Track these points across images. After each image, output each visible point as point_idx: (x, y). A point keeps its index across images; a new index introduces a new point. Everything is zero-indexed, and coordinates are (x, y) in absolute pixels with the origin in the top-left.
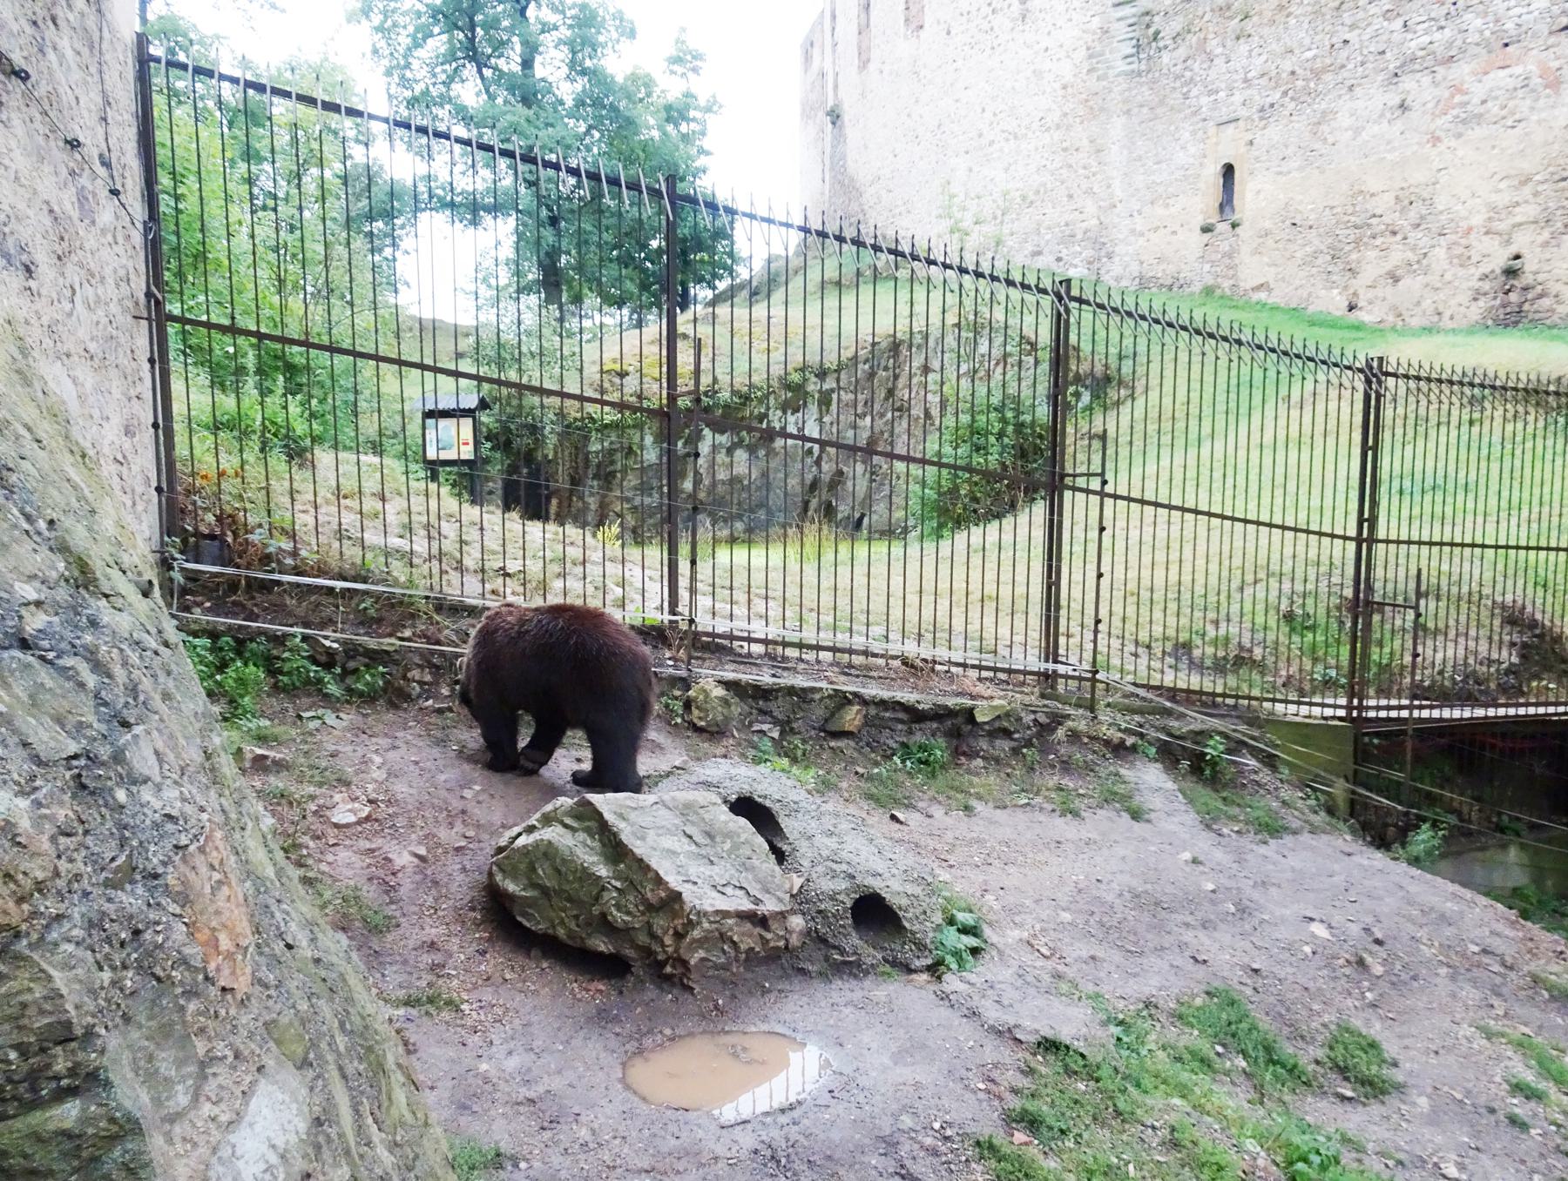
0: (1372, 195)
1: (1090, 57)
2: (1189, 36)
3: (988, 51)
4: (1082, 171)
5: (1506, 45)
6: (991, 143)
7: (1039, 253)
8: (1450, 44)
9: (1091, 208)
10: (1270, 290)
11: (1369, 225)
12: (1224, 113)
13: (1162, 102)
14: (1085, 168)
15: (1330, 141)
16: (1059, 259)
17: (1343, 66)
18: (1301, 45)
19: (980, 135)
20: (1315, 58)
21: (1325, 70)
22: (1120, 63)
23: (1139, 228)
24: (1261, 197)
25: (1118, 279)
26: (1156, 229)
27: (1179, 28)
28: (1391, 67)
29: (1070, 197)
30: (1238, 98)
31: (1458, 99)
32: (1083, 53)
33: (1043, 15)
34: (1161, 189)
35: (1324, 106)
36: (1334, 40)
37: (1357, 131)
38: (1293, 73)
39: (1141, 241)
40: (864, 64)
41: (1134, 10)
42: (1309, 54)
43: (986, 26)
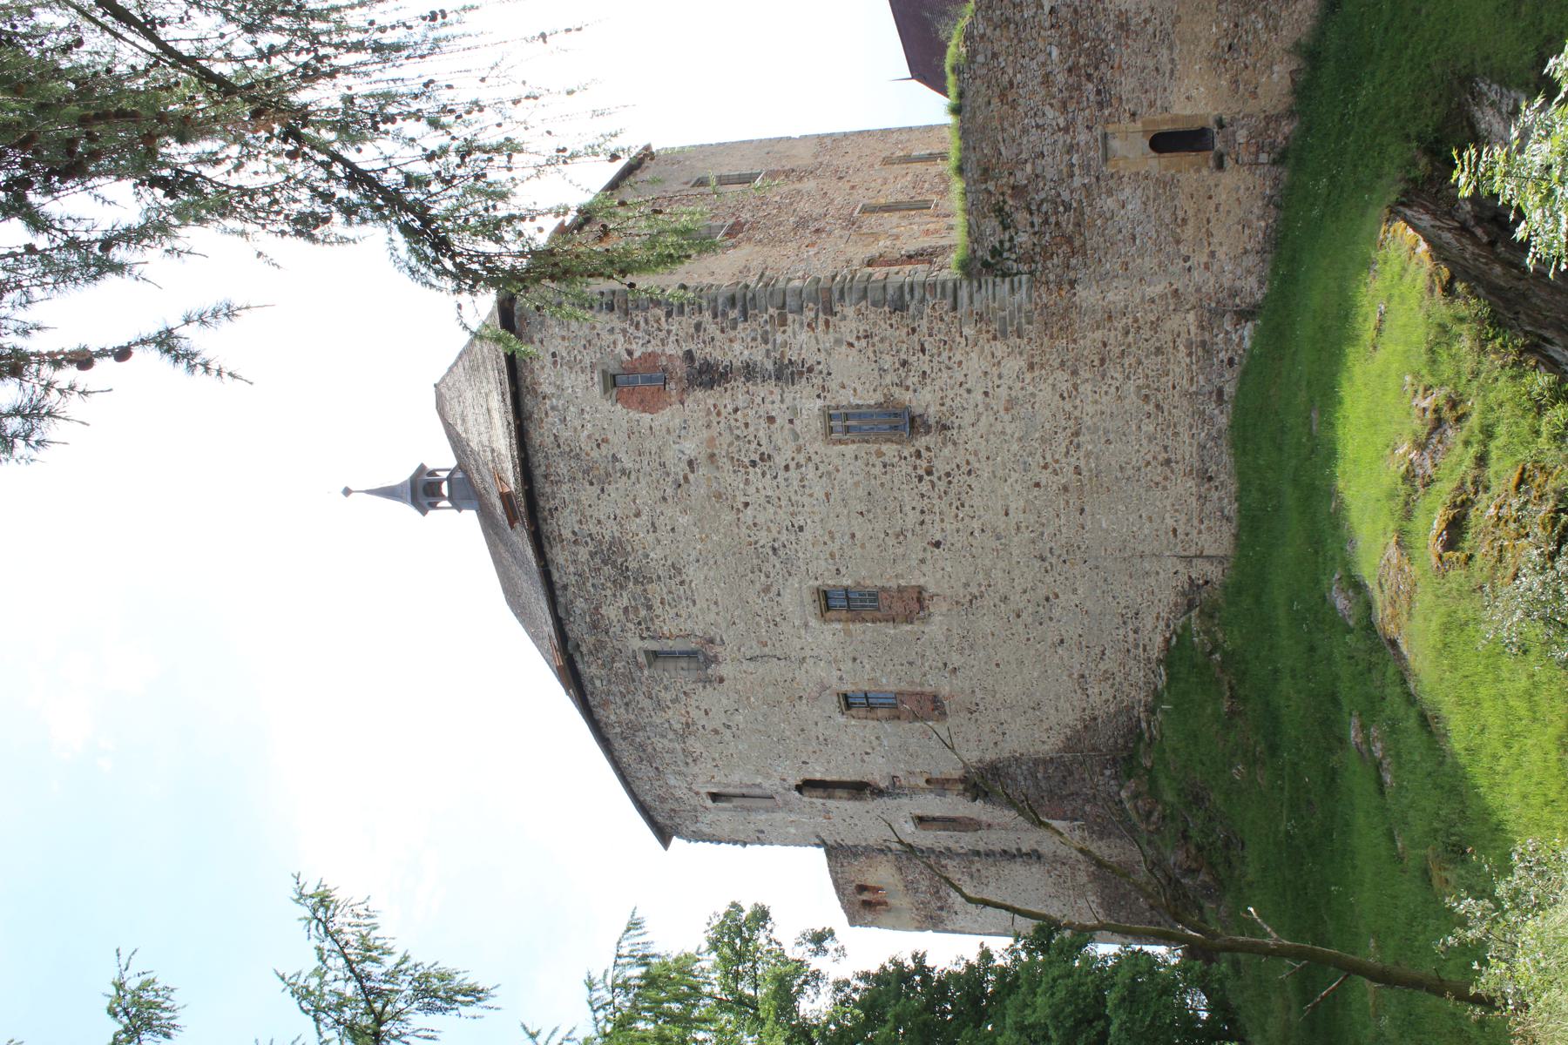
1: (1004, 334)
2: (1007, 208)
3: (971, 480)
4: (1130, 338)
7: (1220, 392)
14: (1127, 333)
15: (1147, 14)
16: (1231, 362)
17: (1076, 11)
18: (1044, 64)
19: (1066, 489)
20: (1059, 45)
22: (1017, 297)
23: (1204, 259)
24: (1194, 93)
25: (1261, 283)
27: (995, 223)
29: (1159, 351)
30: (1083, 137)
32: (1000, 348)
33: (948, 402)
35: (1110, 28)
36: (1047, 24)
38: (1070, 70)
39: (1221, 254)
41: (965, 283)
42: (1055, 52)
43: (942, 485)
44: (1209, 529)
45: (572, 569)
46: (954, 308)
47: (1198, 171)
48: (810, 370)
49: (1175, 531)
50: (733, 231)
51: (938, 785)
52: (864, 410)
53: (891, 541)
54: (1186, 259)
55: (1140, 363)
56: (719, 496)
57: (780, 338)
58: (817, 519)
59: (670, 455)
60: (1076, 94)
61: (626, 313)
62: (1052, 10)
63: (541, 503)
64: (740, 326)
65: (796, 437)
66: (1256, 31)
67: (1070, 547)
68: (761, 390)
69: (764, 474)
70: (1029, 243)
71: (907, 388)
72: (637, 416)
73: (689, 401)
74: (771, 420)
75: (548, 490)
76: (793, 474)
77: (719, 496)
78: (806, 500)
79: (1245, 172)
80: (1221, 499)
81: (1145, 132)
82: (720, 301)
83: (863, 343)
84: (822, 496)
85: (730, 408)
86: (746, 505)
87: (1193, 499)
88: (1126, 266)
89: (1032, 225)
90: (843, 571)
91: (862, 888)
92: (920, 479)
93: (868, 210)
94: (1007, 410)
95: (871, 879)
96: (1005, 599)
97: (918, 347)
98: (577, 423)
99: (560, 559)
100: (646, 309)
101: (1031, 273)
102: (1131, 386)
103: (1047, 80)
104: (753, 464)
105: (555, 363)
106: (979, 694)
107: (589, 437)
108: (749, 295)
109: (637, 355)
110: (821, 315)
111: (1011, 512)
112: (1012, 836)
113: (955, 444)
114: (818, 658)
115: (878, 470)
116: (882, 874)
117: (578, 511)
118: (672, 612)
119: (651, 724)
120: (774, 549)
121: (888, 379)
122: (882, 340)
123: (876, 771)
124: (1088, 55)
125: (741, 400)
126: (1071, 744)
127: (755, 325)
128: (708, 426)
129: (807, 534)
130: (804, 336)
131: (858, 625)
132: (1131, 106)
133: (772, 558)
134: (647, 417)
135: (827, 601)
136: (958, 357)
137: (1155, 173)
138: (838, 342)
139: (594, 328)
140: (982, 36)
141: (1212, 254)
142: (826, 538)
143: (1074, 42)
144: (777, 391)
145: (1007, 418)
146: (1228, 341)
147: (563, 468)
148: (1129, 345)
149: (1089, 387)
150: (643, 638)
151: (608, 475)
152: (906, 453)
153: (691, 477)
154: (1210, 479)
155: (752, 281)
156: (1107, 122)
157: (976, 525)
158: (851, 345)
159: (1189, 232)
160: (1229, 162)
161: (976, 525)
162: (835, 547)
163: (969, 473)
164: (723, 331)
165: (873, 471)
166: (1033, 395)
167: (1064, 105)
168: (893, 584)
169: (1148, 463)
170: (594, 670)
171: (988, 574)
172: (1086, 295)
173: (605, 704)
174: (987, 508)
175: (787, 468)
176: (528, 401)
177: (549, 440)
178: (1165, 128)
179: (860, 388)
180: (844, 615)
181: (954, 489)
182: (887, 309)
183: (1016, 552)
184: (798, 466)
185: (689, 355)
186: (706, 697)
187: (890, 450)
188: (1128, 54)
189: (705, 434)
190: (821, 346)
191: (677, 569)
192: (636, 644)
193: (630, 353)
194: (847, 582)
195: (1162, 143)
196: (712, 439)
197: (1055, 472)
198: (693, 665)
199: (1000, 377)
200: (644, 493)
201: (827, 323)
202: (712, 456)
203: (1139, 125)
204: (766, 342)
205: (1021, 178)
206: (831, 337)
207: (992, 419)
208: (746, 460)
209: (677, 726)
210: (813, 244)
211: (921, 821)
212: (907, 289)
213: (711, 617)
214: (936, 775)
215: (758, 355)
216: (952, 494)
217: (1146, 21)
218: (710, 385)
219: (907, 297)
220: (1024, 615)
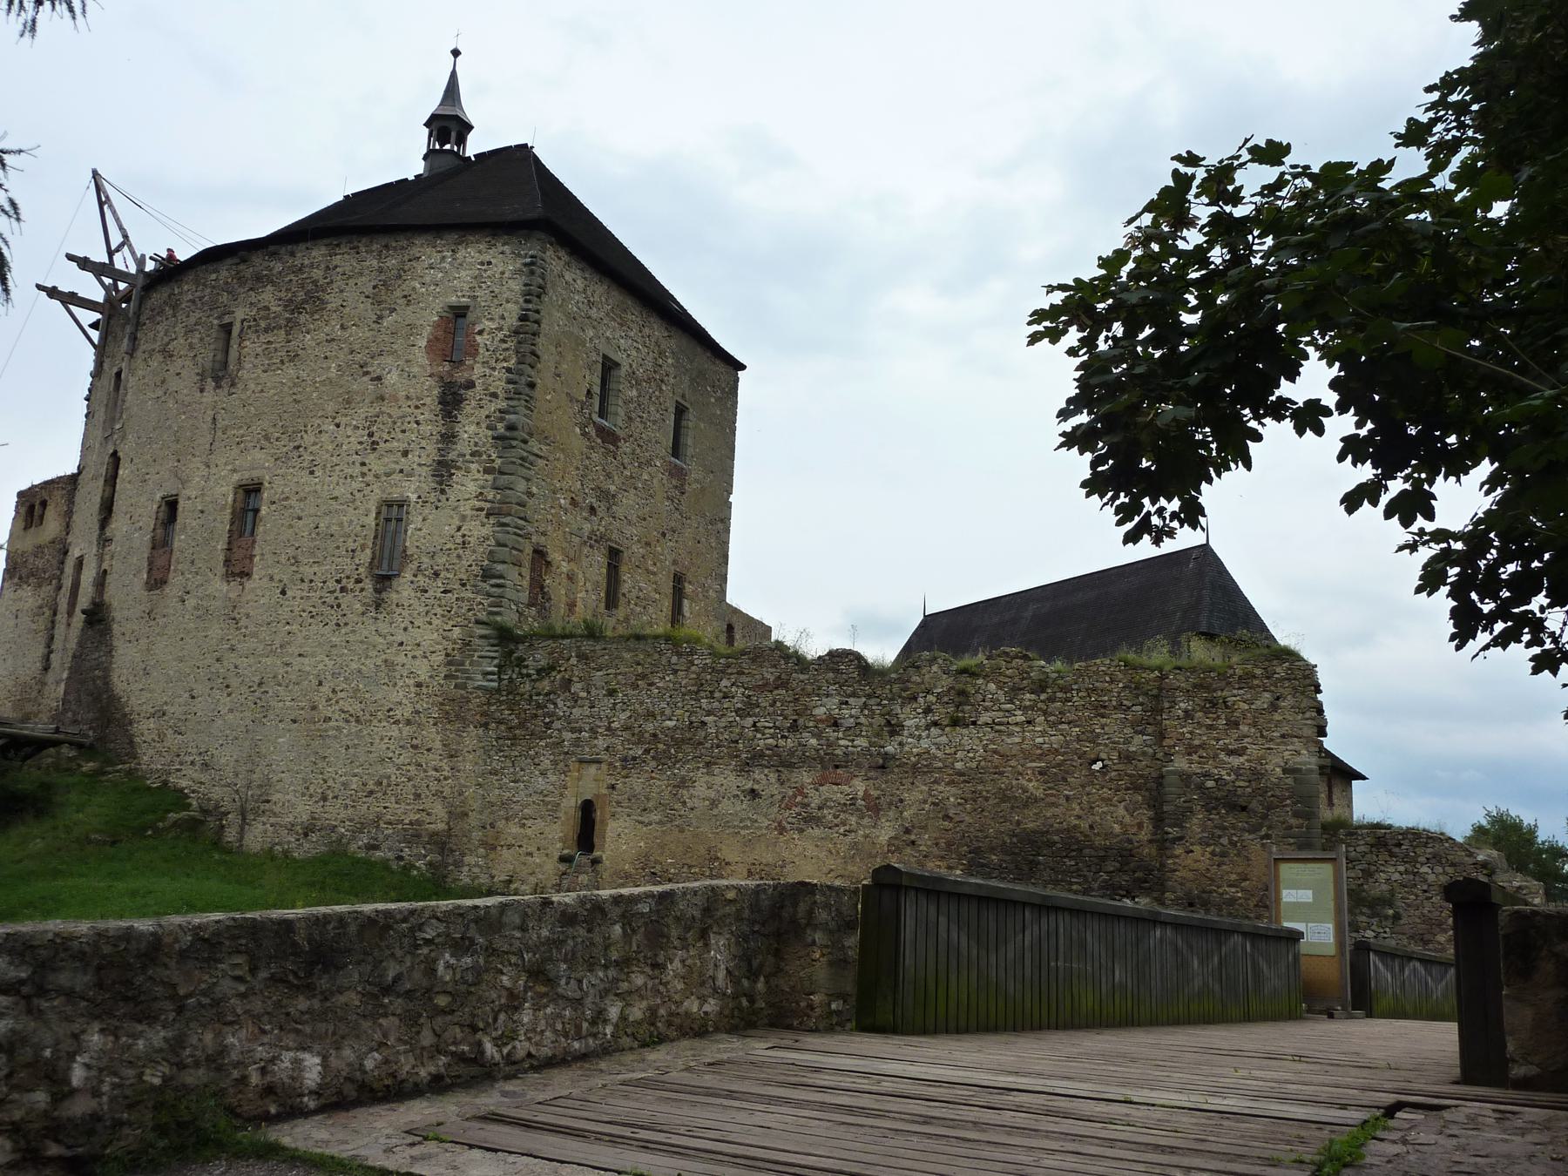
1: (450, 663)
5: (837, 767)
8: (792, 753)
12: (587, 752)
13: (522, 725)
16: (400, 858)
18: (662, 713)
19: (314, 708)
27: (543, 663)
29: (417, 796)
30: (601, 743)
31: (799, 799)
32: (439, 658)
33: (399, 610)
34: (517, 807)
37: (714, 803)
38: (655, 735)
40: (157, 582)
43: (330, 600)
44: (265, 832)
45: (306, 262)
46: (478, 622)
47: (561, 840)
48: (443, 492)
50: (608, 437)
53: (291, 551)
55: (409, 780)
57: (474, 466)
61: (516, 332)
62: (704, 723)
65: (388, 475)
67: (266, 709)
70: (522, 690)
72: (425, 334)
73: (430, 382)
74: (405, 454)
75: (375, 247)
76: (357, 470)
78: (334, 479)
81: (597, 796)
82: (512, 417)
83: (459, 540)
84: (336, 493)
86: (338, 426)
87: (291, 819)
88: (494, 772)
89: (538, 694)
90: (273, 507)
91: (44, 504)
92: (338, 581)
93: (614, 555)
96: (232, 649)
98: (427, 279)
99: (314, 253)
101: (498, 691)
102: (391, 770)
103: (651, 715)
104: (371, 435)
105: (482, 264)
106: (161, 621)
107: (414, 289)
108: (514, 443)
109: (478, 338)
110: (488, 505)
114: (207, 480)
115: (351, 545)
116: (52, 526)
117: (351, 272)
118: (259, 350)
121: (425, 560)
122: (459, 557)
123: (119, 525)
125: (426, 429)
126: (114, 699)
128: (408, 398)
129: (305, 477)
130: (472, 488)
131: (228, 517)
133: (292, 445)
134: (423, 343)
135: (251, 490)
136: (436, 622)
138: (463, 518)
147: (392, 262)
149: (395, 734)
151: (380, 303)
152: (361, 570)
153: (366, 379)
155: (534, 446)
156: (610, 764)
157: (295, 627)
158: (459, 529)
159: (515, 830)
160: (563, 867)
161: (295, 627)
162: (293, 502)
167: (627, 728)
168: (257, 551)
170: (224, 273)
172: (471, 738)
173: (197, 283)
174: (306, 638)
175: (363, 464)
177: (415, 251)
179: (421, 533)
180: (239, 505)
183: (269, 661)
184: (363, 475)
185: (470, 385)
186: (190, 375)
188: (661, 785)
192: (240, 314)
193: (481, 332)
194: (264, 511)
196: (397, 400)
198: (217, 366)
200: (362, 333)
201: (481, 509)
202: (383, 399)
203: (604, 791)
205: (576, 687)
206: (469, 513)
211: (80, 562)
213: (252, 386)
214: (109, 579)
215: (463, 446)
216: (323, 608)
217: (684, 803)
218: (443, 401)
219: (493, 581)
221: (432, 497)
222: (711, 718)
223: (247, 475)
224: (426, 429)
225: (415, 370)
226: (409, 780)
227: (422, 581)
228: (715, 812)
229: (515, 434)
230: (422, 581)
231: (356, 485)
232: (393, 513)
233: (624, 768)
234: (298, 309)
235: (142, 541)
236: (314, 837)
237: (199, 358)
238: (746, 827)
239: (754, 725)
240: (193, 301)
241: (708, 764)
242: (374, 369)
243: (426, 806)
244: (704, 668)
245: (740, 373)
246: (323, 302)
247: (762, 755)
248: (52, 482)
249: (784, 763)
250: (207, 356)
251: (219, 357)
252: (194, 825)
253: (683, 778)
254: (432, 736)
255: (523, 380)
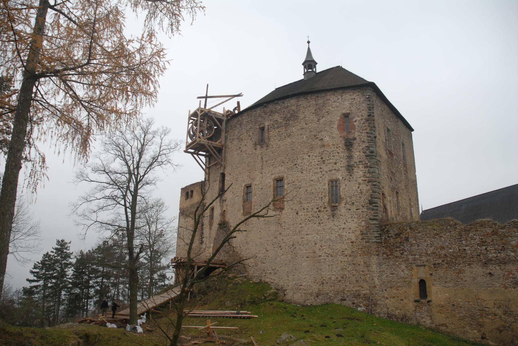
0: (484, 300)
1: (362, 234)
2: (401, 235)
6: (320, 256)
7: (345, 300)
9: (365, 285)
10: (447, 327)
11: (485, 310)
15: (464, 279)
16: (353, 303)
18: (447, 247)
19: (314, 252)
20: (454, 252)
21: (458, 256)
22: (373, 238)
23: (386, 296)
25: (379, 313)
26: (394, 297)
28: (484, 261)
29: (357, 281)
30: (424, 258)
31: (511, 276)
33: (341, 217)
34: (394, 283)
37: (474, 279)
39: (387, 301)
43: (315, 215)
44: (302, 296)
46: (370, 219)
47: (413, 294)
48: (351, 175)
49: (301, 285)
51: (223, 214)
52: (338, 192)
54: (386, 290)
55: (353, 275)
56: (312, 148)
58: (305, 177)
59: (324, 133)
60: (438, 257)
62: (465, 250)
63: (309, 95)
64: (364, 154)
65: (330, 171)
66: (459, 313)
68: (344, 161)
69: (319, 161)
71: (345, 205)
73: (341, 139)
74: (335, 164)
75: (313, 97)
76: (319, 170)
77: (312, 148)
78: (311, 174)
79: (414, 308)
80: (311, 299)
82: (372, 149)
84: (312, 179)
85: (339, 151)
86: (309, 156)
87: (311, 291)
89: (396, 243)
90: (289, 185)
92: (317, 209)
94: (339, 235)
95: (195, 193)
96: (280, 234)
97: (358, 208)
98: (334, 106)
100: (369, 126)
102: (346, 273)
103: (442, 248)
104: (322, 158)
105: (352, 99)
106: (251, 226)
109: (355, 123)
111: (307, 236)
112: (208, 236)
113: (328, 219)
115: (320, 196)
116: (196, 198)
117: (306, 107)
118: (276, 134)
119: (242, 129)
120: (295, 165)
121: (348, 199)
122: (360, 197)
124: (450, 261)
125: (341, 155)
127: (364, 159)
128: (333, 145)
129: (300, 174)
130: (361, 173)
132: (434, 274)
134: (336, 126)
136: (355, 220)
137: (413, 281)
138: (359, 184)
139: (363, 110)
140: (456, 228)
141: (387, 298)
142: (299, 180)
143: (454, 256)
144: (344, 165)
145: (337, 235)
146: (360, 302)
147: (320, 102)
148: (359, 272)
150: (268, 126)
151: (318, 115)
152: (325, 204)
153: (317, 140)
154: (317, 296)
155: (378, 158)
156: (429, 266)
158: (359, 188)
159: (395, 291)
160: (416, 304)
162: (296, 183)
163: (319, 223)
164: (362, 149)
165: (320, 194)
166: (343, 243)
167: (434, 253)
169: (322, 278)
171: (288, 229)
172: (374, 260)
175: (321, 168)
176: (341, 91)
177: (328, 97)
178: (427, 284)
180: (275, 185)
181: (314, 219)
182: (370, 198)
183: (295, 237)
185: (355, 139)
186: (250, 144)
187: (326, 199)
189: (331, 144)
190: (358, 179)
191: (289, 136)
192: (267, 124)
193: (355, 121)
194: (286, 186)
195: (422, 283)
196: (329, 146)
197: (319, 249)
199: (349, 233)
201: (365, 180)
202: (324, 146)
204: (359, 162)
206: (361, 182)
207: (336, 230)
208: (323, 156)
209: (241, 137)
210: (388, 177)
212: (376, 205)
213: (275, 146)
216: (313, 218)
217: (462, 279)
219: (374, 205)
220: (275, 240)
221: (347, 178)
222: (467, 248)
223: (277, 175)
224: (341, 155)
225: (334, 135)
226: (353, 275)
227: (348, 206)
228: (476, 281)
229: (373, 154)
230: (348, 206)
231: (319, 175)
232: (334, 184)
233: (435, 267)
234: (289, 120)
235: (239, 200)
236: (320, 297)
237: (253, 139)
238: (490, 287)
239: (486, 249)
240: (248, 122)
241: (469, 264)
242: (319, 136)
243: (361, 285)
244: (461, 230)
245: (412, 133)
246: (297, 116)
247: (491, 260)
248: (194, 184)
249: (503, 262)
250: (256, 138)
251: (260, 138)
252: (276, 294)
253: (460, 270)
254: (360, 260)
255: (373, 136)
